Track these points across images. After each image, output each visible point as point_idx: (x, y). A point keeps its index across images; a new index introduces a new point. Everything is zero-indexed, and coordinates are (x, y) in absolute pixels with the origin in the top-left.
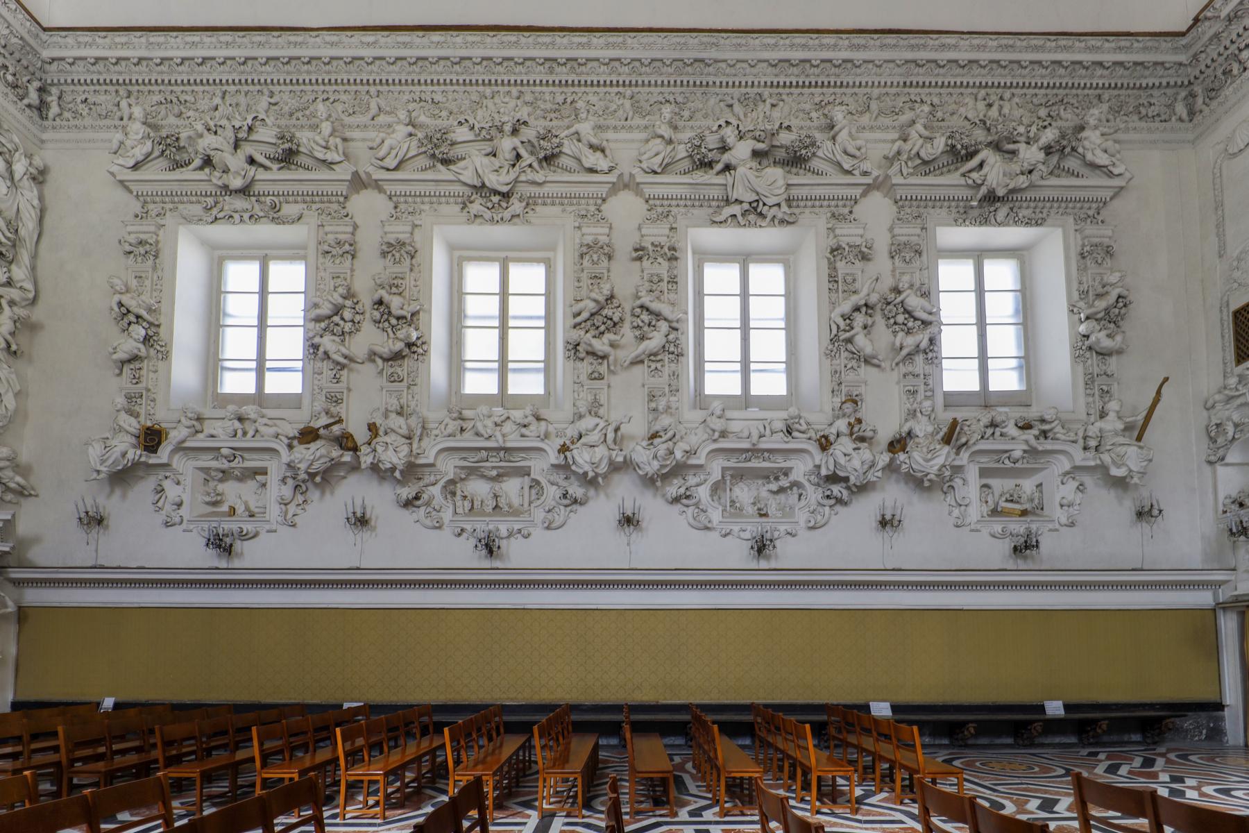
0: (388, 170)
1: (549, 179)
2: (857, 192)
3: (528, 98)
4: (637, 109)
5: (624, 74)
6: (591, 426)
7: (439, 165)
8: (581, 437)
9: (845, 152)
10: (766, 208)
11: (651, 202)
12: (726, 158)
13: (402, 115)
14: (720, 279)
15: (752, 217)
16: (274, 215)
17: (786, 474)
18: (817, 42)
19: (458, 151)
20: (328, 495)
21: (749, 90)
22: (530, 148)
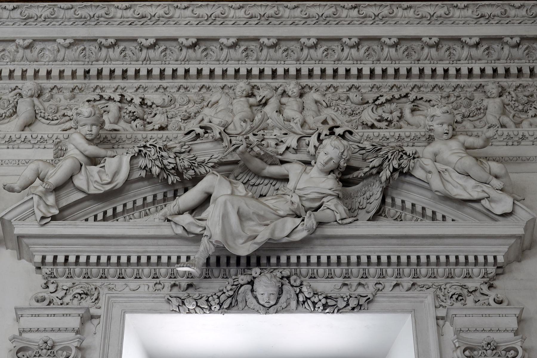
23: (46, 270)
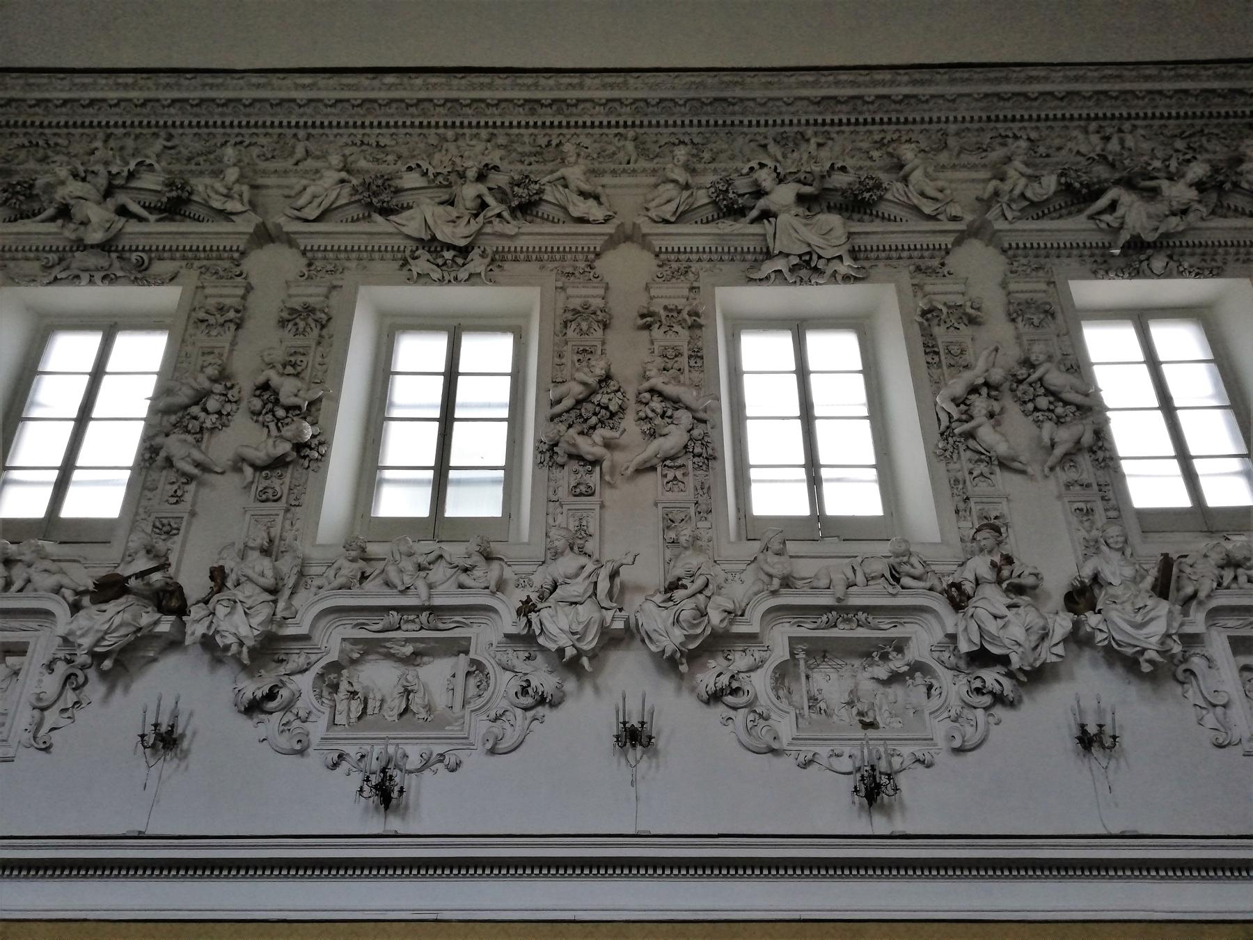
0: (306, 221)
1: (522, 230)
2: (948, 240)
3: (502, 140)
4: (643, 151)
5: (626, 115)
6: (571, 570)
7: (377, 218)
8: (555, 587)
9: (923, 194)
10: (822, 262)
11: (662, 256)
12: (762, 203)
13: (335, 160)
14: (764, 353)
15: (804, 273)
16: (141, 273)
17: (899, 650)
18: (868, 78)
19: (406, 199)
20: (119, 691)
21: (787, 129)
22: (499, 196)
23: (1010, 253)
